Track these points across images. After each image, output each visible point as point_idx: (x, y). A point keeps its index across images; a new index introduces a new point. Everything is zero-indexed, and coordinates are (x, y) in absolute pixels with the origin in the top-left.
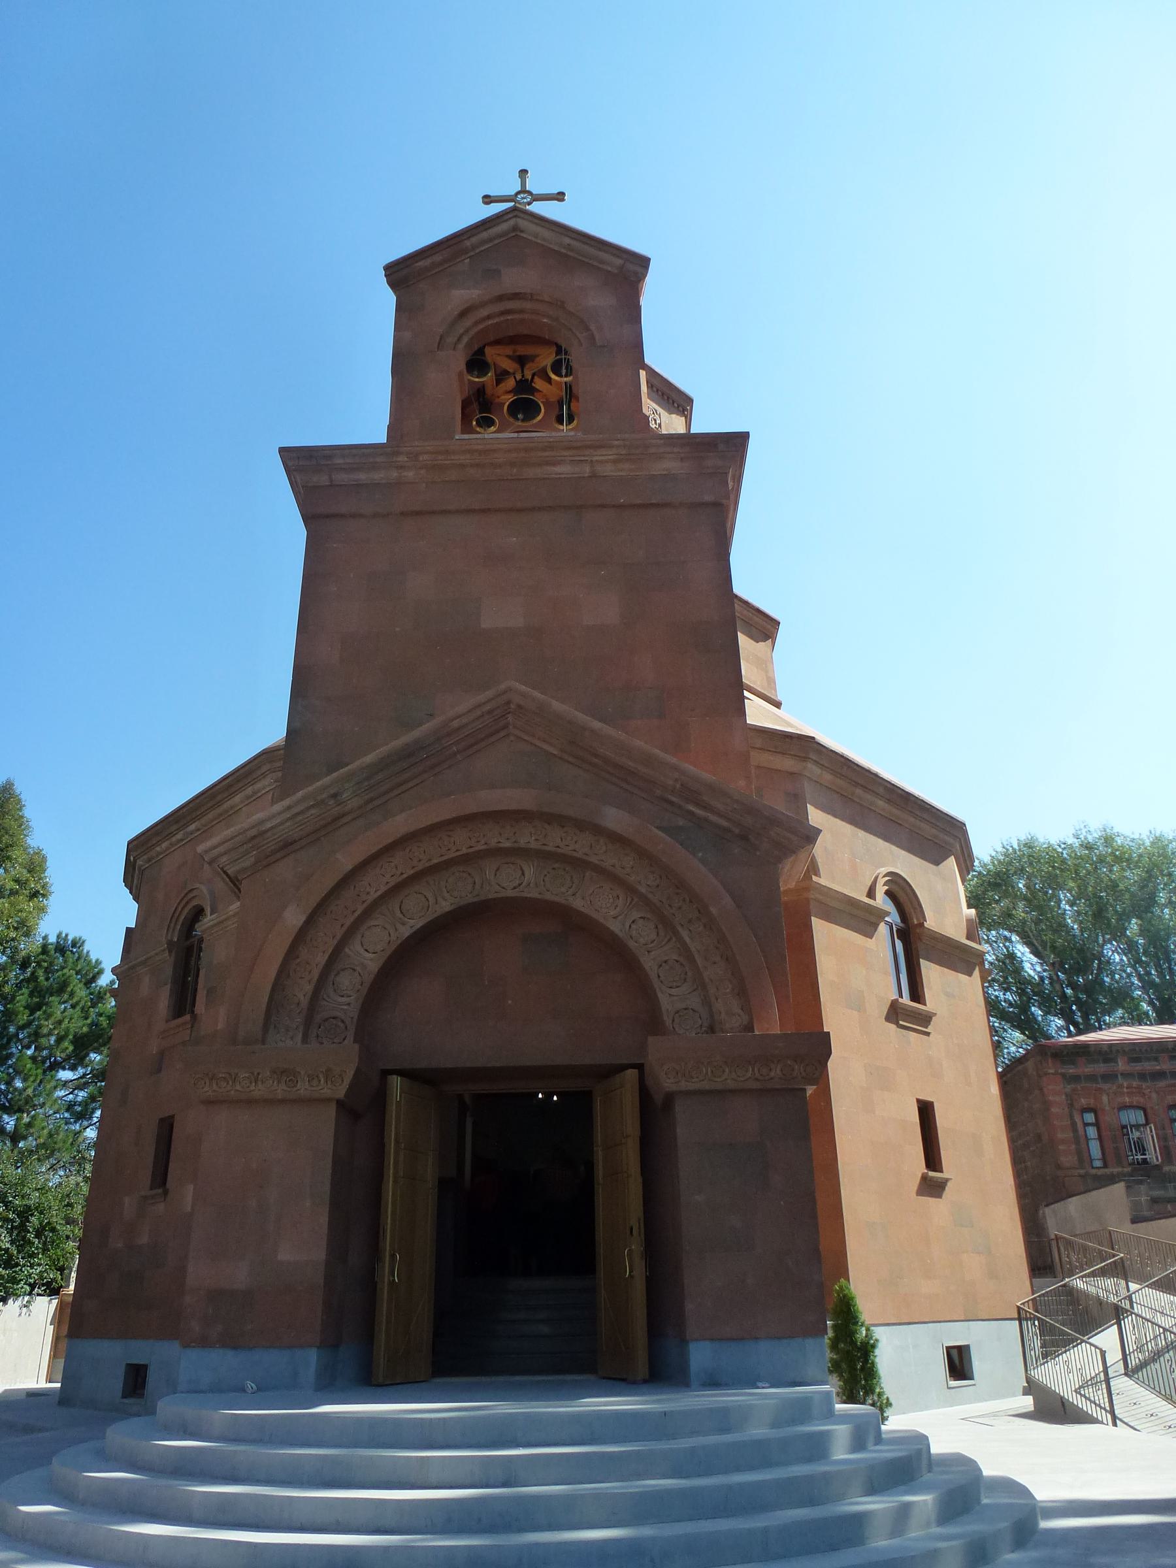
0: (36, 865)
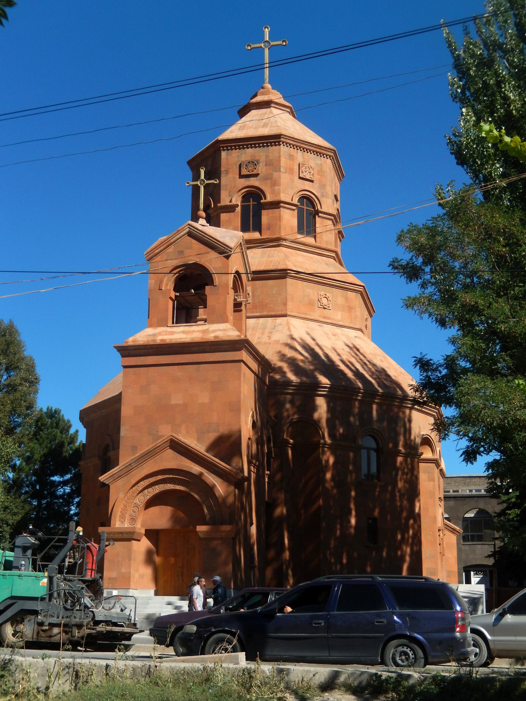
0: (31, 368)
